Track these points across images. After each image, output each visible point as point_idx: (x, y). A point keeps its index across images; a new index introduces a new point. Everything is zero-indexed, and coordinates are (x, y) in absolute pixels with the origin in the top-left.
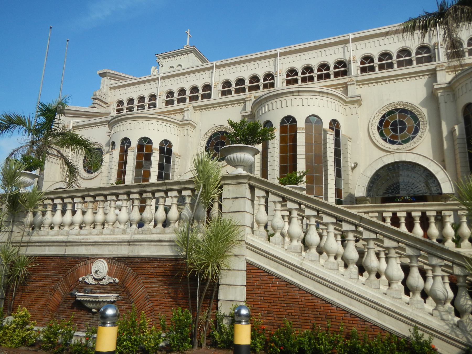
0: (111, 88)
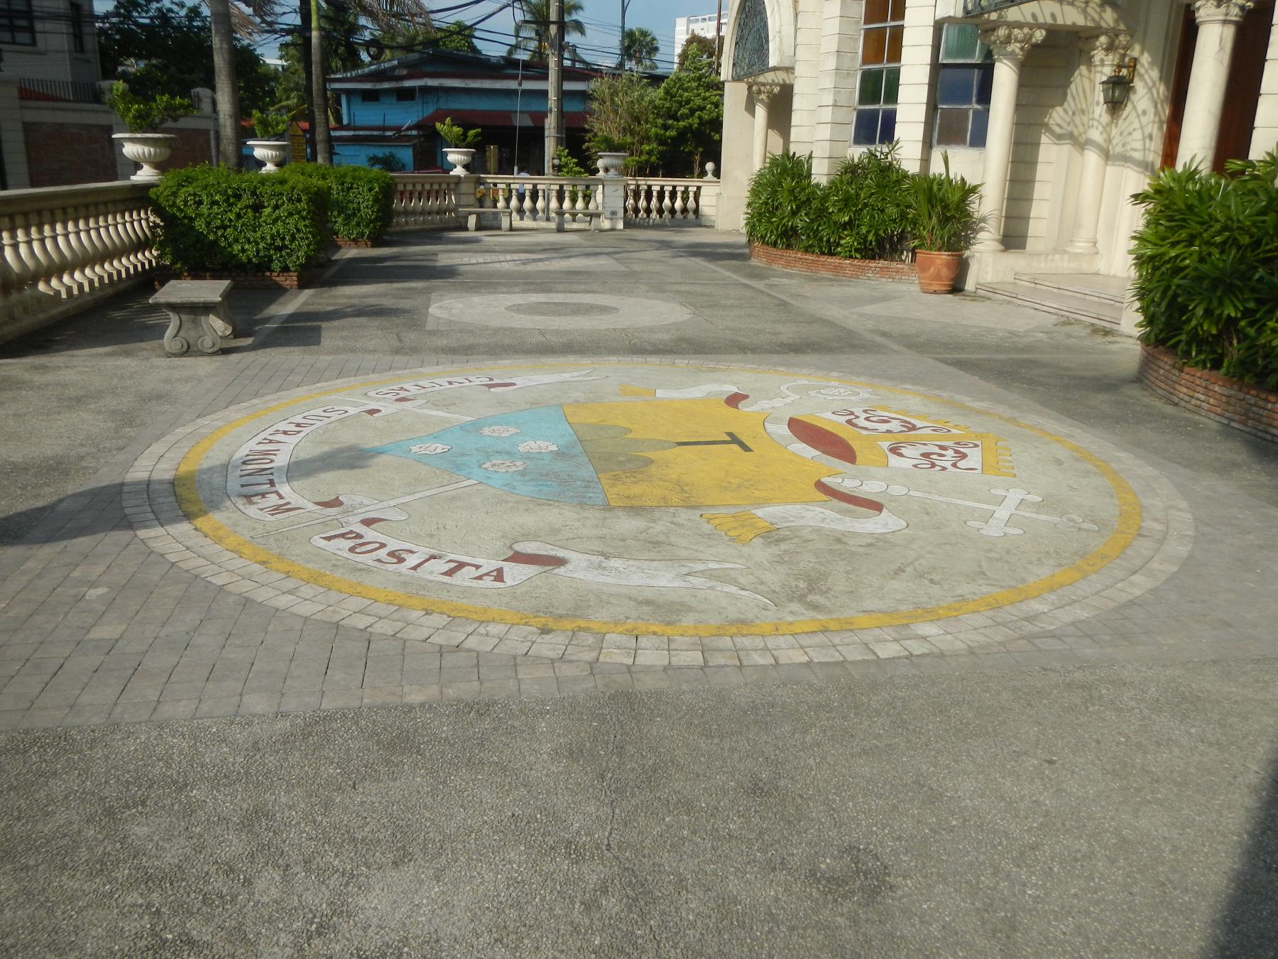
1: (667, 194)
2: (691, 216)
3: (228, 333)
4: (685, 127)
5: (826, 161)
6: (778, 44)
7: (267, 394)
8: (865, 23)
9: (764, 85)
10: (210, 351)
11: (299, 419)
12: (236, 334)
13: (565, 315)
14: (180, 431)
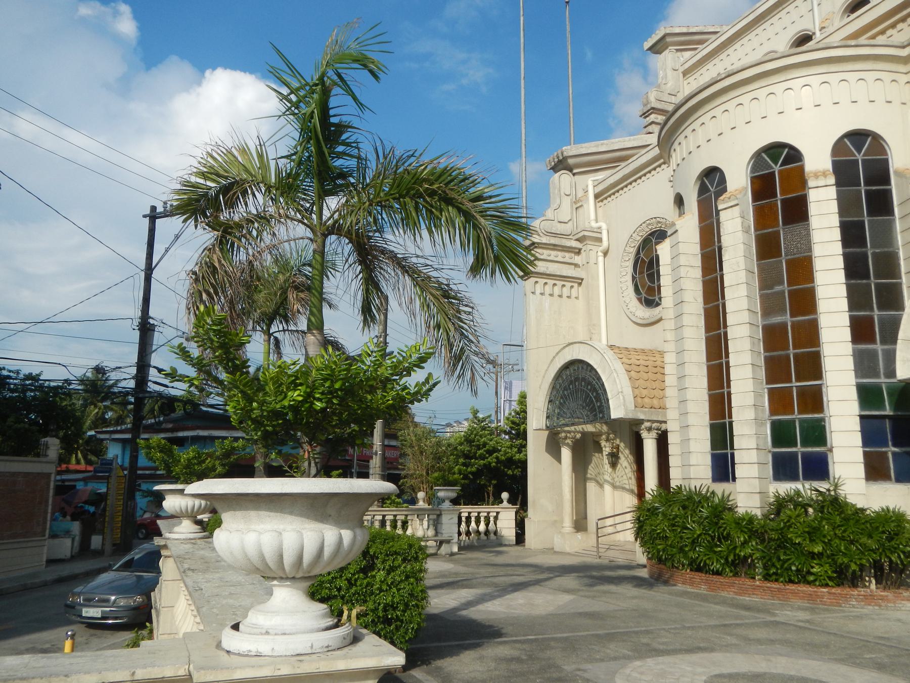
0: (685, 73)
1: (473, 519)
2: (492, 536)
4: (485, 465)
5: (758, 495)
6: (622, 401)
8: (767, 383)
9: (569, 432)
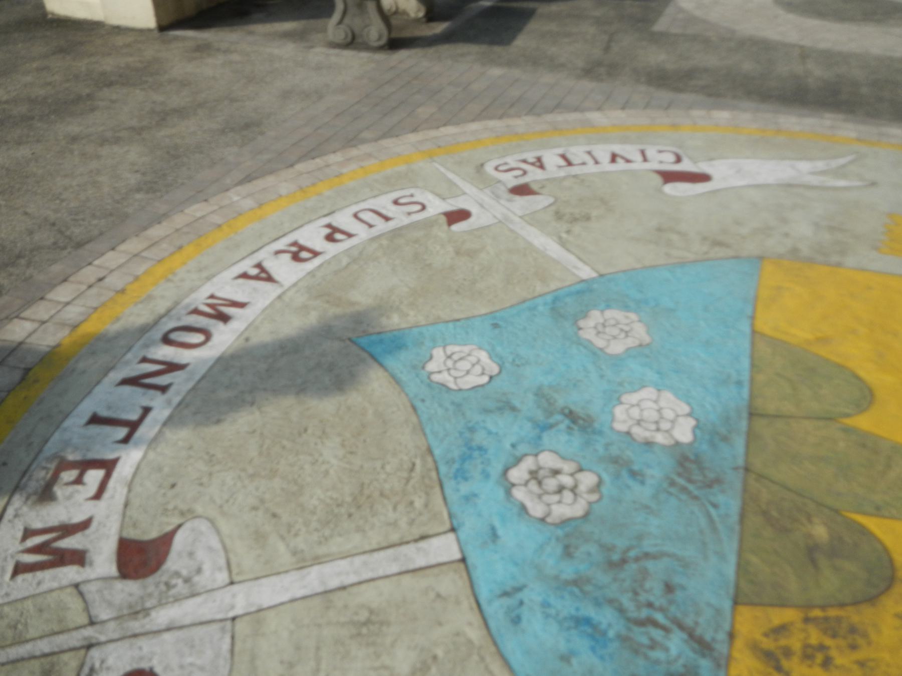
3: (421, 14)
7: (364, 141)
10: (376, 44)
11: (343, 220)
12: (431, 16)
13: (852, 19)
14: (196, 210)
